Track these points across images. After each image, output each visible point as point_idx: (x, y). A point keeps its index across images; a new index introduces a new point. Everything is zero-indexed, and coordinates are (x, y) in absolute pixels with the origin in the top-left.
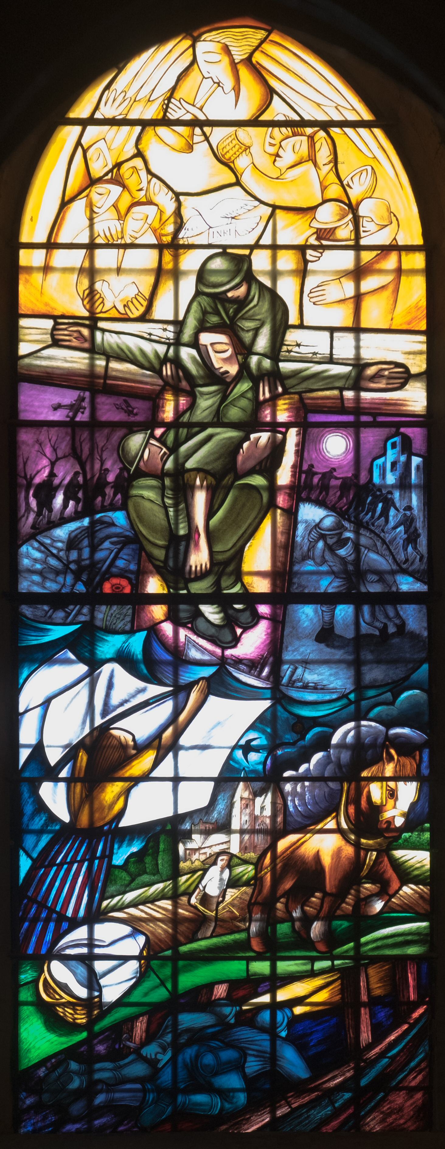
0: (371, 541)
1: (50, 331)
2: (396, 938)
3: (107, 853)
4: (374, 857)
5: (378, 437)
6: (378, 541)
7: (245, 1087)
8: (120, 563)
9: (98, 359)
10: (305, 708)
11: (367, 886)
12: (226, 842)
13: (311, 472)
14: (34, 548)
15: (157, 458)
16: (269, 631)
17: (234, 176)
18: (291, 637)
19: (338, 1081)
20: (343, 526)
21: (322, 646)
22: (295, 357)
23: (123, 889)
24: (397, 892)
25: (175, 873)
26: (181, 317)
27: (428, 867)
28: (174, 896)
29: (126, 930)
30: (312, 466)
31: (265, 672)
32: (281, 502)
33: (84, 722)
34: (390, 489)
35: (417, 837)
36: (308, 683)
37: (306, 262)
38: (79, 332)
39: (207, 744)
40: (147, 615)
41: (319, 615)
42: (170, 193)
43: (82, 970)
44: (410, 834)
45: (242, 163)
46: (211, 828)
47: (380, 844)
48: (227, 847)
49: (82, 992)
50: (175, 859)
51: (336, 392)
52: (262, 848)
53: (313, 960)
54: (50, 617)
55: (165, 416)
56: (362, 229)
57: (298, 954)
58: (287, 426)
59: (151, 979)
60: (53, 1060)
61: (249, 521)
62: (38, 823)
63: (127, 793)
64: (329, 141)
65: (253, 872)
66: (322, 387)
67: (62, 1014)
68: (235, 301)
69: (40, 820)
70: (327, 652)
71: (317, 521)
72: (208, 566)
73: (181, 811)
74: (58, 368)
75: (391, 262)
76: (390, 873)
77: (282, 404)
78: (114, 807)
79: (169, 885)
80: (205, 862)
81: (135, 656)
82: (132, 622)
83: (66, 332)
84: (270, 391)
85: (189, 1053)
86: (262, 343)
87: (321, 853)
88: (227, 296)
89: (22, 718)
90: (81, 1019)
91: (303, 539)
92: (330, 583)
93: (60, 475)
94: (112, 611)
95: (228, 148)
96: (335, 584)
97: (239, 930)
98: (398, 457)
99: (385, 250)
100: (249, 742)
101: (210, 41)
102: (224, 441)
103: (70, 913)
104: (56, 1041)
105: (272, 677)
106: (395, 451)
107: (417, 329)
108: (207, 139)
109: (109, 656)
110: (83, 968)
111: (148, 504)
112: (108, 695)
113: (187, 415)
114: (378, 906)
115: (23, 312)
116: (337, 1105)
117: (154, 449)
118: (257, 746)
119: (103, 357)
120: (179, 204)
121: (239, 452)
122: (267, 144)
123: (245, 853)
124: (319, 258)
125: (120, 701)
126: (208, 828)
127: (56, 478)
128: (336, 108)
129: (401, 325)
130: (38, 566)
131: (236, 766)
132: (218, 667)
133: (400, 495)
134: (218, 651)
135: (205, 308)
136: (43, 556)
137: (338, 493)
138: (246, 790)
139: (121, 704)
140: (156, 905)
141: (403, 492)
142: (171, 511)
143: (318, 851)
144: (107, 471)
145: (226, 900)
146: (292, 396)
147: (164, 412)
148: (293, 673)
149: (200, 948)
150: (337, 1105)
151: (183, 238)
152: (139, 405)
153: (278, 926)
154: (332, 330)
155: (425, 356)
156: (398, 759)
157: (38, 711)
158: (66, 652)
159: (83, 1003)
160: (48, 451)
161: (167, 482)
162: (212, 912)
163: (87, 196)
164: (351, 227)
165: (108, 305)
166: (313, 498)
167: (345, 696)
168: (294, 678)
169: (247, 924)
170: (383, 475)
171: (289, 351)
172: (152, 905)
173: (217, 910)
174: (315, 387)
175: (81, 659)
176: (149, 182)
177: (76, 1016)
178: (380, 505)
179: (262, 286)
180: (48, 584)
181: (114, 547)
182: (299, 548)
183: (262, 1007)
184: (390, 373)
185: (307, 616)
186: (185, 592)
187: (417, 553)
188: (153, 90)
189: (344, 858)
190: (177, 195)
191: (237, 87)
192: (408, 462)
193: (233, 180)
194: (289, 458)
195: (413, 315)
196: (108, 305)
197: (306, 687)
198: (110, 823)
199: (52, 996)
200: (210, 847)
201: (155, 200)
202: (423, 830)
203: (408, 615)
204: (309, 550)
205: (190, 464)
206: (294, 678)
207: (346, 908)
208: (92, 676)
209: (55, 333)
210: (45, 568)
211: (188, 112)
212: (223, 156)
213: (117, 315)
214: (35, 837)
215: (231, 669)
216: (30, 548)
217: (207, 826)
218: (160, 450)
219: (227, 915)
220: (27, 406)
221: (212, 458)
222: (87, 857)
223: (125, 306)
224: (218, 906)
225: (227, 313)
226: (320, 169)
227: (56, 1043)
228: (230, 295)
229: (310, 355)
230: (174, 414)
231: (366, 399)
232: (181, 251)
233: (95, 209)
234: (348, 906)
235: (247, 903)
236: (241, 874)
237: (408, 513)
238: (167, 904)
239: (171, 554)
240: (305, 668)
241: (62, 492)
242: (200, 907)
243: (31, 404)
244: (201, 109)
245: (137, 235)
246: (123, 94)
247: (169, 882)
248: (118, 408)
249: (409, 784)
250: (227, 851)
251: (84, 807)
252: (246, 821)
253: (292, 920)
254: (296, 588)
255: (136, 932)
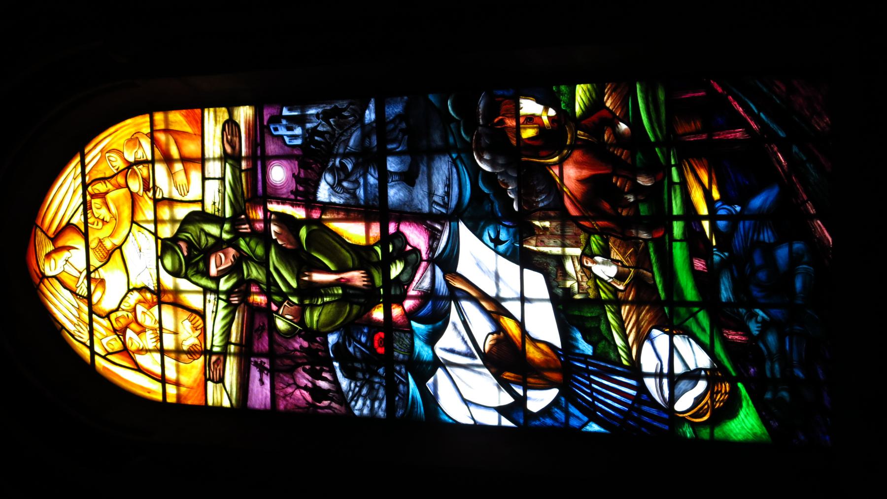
0: (341, 144)
1: (215, 384)
2: (651, 110)
3: (583, 359)
4: (582, 133)
5: (271, 142)
6: (341, 139)
7: (787, 243)
8: (363, 339)
9: (230, 350)
10: (464, 193)
11: (606, 138)
12: (572, 259)
13: (296, 192)
14: (356, 405)
15: (291, 309)
16: (407, 223)
17: (116, 250)
18: (411, 206)
19: (781, 158)
20: (331, 166)
21: (417, 181)
22: (222, 206)
23: (612, 347)
24: (611, 111)
25: (598, 302)
26: (201, 289)
27: (589, 86)
28: (617, 303)
29: (647, 345)
30: (292, 192)
31: (438, 227)
32: (317, 215)
33: (480, 373)
34: (305, 131)
35: (565, 96)
36: (445, 192)
37: (163, 199)
38: (214, 363)
39: (494, 274)
40: (400, 320)
41: (395, 184)
42: (129, 295)
43: (683, 385)
44: (562, 102)
45: (108, 244)
46: (560, 271)
47: (570, 128)
48: (576, 258)
49: (702, 385)
50: (586, 301)
51: (243, 175)
52: (577, 229)
53: (671, 184)
54: (403, 395)
55: (263, 302)
56: (142, 159)
57: (666, 196)
58: (266, 211)
59: (689, 325)
60: (764, 413)
61: (331, 240)
62: (559, 414)
63: (534, 341)
64: (93, 184)
65: (597, 236)
66: (240, 185)
67: (722, 404)
68: (189, 251)
69: (558, 413)
70: (422, 178)
71: (328, 187)
72: (363, 272)
73: (547, 296)
74: (237, 380)
75: (162, 137)
76: (594, 118)
77: (253, 215)
78: (546, 352)
79: (608, 307)
80: (589, 277)
81: (431, 331)
82: (405, 332)
83: (215, 373)
84: (245, 224)
85: (756, 293)
86: (214, 230)
87: (580, 178)
88: (187, 256)
89: (478, 422)
90: (726, 387)
91: (341, 197)
92: (372, 176)
93: (305, 382)
94: (398, 347)
95: (101, 254)
96: (372, 171)
97: (646, 248)
98: (283, 125)
99: (154, 142)
100: (492, 240)
101: (44, 266)
102: (278, 259)
103: (633, 392)
104: (746, 410)
105: (441, 222)
106: (279, 128)
107: (200, 116)
108: (97, 269)
109: (430, 351)
110: (681, 383)
111: (323, 317)
112: (459, 353)
113: (263, 286)
114: (623, 127)
115: (204, 402)
116: (804, 158)
117: (285, 312)
118: (495, 233)
119: (229, 347)
120: (135, 289)
121: (284, 247)
122: (97, 227)
123: (581, 243)
124: (160, 189)
125: (463, 343)
126: (561, 274)
127: (308, 385)
128: (75, 179)
129: (198, 128)
130: (368, 402)
131: (510, 250)
132: (435, 265)
133: (309, 123)
134: (424, 264)
135: (194, 272)
136: (360, 398)
137: (309, 171)
138: (530, 243)
139: (466, 343)
140: (626, 319)
141: (307, 121)
142: (327, 299)
143: (578, 181)
144: (301, 347)
145: (620, 259)
146: (247, 207)
147: (261, 303)
148: (438, 204)
149: (662, 282)
150: (804, 158)
151: (154, 287)
152: (259, 321)
153: (642, 214)
154: (204, 179)
155: (217, 109)
156: (501, 116)
157: (472, 408)
158: (428, 384)
159: (711, 385)
160: (290, 390)
161: (307, 302)
162: (631, 271)
163: (133, 353)
164: (141, 167)
165: (196, 342)
166: (313, 190)
167: (454, 162)
168: (442, 203)
169: (641, 241)
170: (295, 137)
171: (219, 210)
172: (625, 323)
173: (629, 267)
174: (240, 191)
175: (433, 373)
176: (123, 310)
177: (723, 391)
178: (316, 138)
179: (180, 230)
180: (380, 396)
181: (352, 344)
182: (348, 201)
183: (713, 227)
184: (229, 134)
185: (396, 193)
186: (382, 290)
187: (348, 108)
188: (73, 305)
189: (583, 158)
190: (129, 291)
191: (68, 248)
192: (287, 117)
193: (118, 250)
194: (287, 209)
195: (191, 119)
196: (196, 342)
197: (448, 194)
198: (559, 356)
199: (705, 411)
200: (576, 272)
201: (133, 305)
202: (559, 91)
203: (393, 113)
204: (349, 193)
205: (294, 284)
206: (442, 203)
207: (625, 155)
208: (445, 365)
209: (215, 380)
210: (369, 397)
211: (83, 282)
212: (105, 258)
213: (202, 335)
214: (571, 418)
215: (437, 254)
216: (357, 407)
217: (559, 275)
218: (286, 307)
219: (633, 259)
220: (262, 404)
221: (289, 268)
222: (586, 375)
223: (196, 330)
224: (625, 266)
225: (197, 256)
226: (109, 190)
227: (747, 410)
228: (186, 254)
229: (220, 194)
230: (262, 296)
231: (247, 152)
232: (161, 288)
233: (141, 348)
234: (622, 154)
235: (622, 241)
236: (598, 246)
237: (321, 116)
238: (625, 310)
239: (356, 300)
240: (434, 194)
241: (317, 381)
242: (627, 282)
243: (260, 400)
244: (81, 273)
245: (154, 320)
246: (76, 326)
247: (607, 308)
248: (261, 337)
249: (521, 106)
250: (579, 258)
251: (546, 376)
252: (554, 242)
253: (636, 202)
254: (376, 202)
255: (649, 337)
